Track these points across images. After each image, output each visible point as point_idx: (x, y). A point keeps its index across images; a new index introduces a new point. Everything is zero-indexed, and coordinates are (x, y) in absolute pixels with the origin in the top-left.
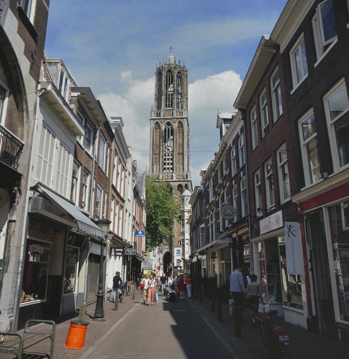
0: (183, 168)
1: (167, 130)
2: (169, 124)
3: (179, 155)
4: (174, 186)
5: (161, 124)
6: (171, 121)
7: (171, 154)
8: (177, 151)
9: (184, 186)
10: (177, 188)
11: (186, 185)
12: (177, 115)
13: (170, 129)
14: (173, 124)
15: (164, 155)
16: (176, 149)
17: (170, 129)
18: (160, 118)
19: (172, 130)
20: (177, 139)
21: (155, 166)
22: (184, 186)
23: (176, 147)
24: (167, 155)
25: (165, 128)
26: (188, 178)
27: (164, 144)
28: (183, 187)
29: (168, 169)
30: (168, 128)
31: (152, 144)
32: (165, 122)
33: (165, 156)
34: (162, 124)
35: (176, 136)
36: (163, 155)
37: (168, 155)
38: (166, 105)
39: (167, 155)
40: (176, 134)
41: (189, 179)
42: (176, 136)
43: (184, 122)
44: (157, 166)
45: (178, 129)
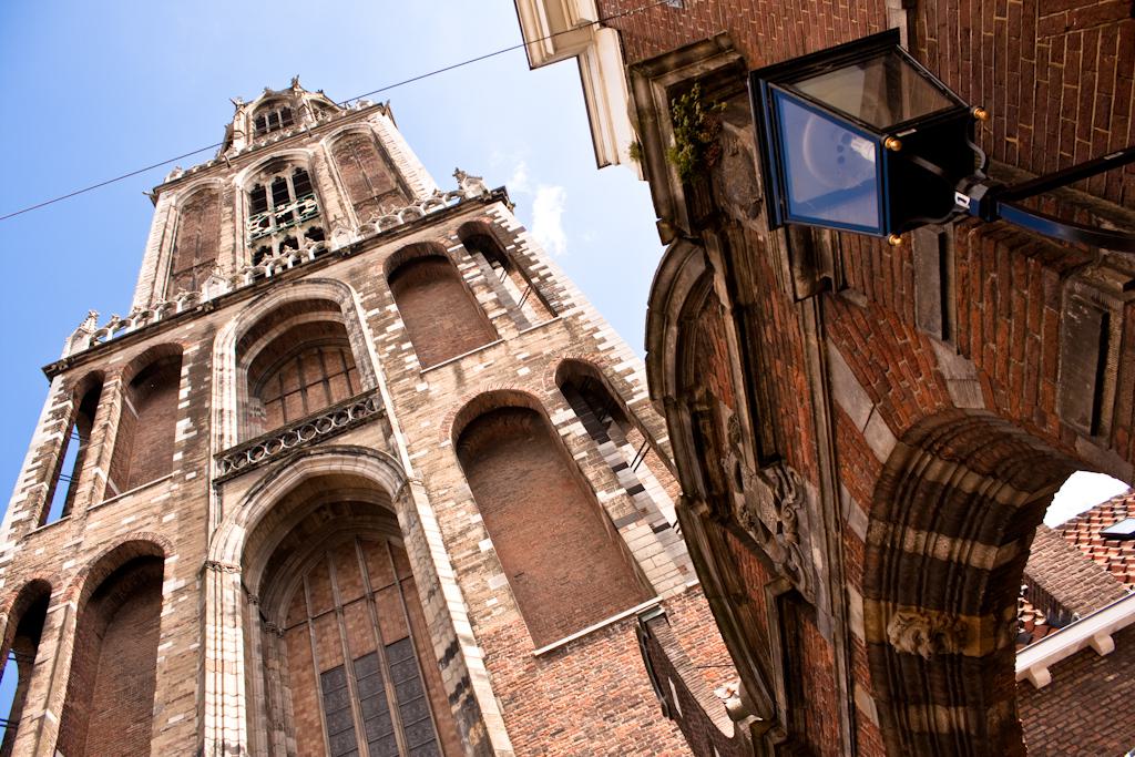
25: (257, 186)
32: (255, 164)
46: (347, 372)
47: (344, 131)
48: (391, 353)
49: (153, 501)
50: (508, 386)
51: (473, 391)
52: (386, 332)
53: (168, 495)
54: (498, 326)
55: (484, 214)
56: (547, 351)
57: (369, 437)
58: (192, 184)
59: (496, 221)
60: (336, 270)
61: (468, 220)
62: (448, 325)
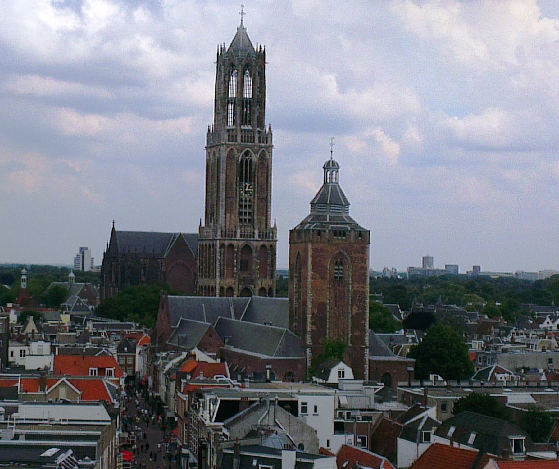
2: (247, 154)
4: (256, 247)
9: (268, 248)
12: (260, 142)
13: (249, 161)
14: (255, 154)
17: (249, 161)
18: (236, 143)
19: (251, 160)
22: (268, 248)
24: (244, 199)
26: (274, 238)
29: (245, 220)
37: (246, 201)
38: (242, 121)
39: (244, 199)
41: (275, 239)
51: (263, 286)
60: (255, 243)
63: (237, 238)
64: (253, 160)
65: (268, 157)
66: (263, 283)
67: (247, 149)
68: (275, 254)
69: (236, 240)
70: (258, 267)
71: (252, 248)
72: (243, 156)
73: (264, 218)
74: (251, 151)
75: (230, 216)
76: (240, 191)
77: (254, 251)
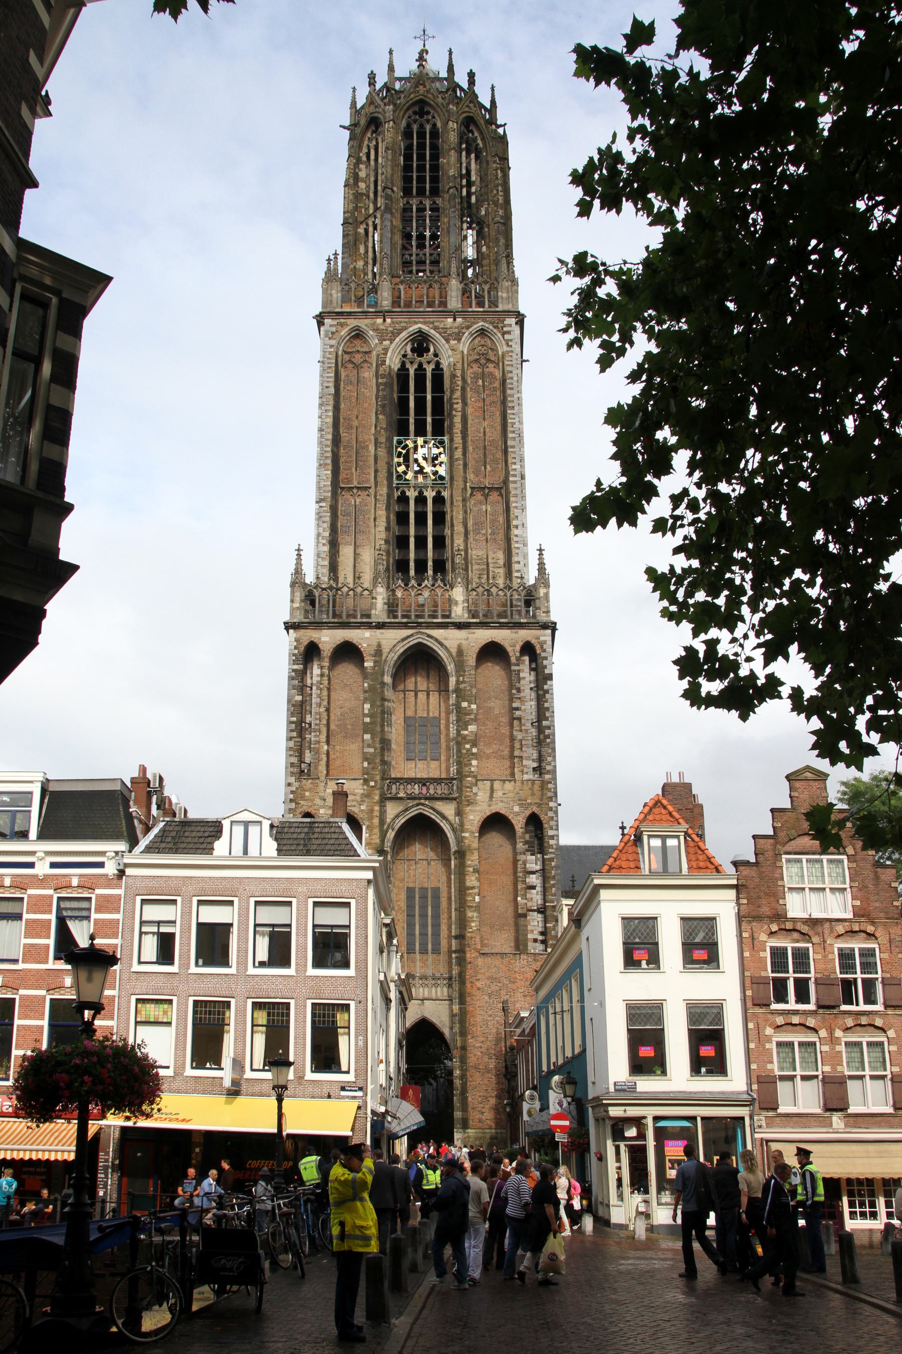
0: (508, 565)
1: (412, 372)
2: (421, 344)
3: (479, 496)
4: (460, 652)
5: (381, 340)
6: (435, 328)
7: (439, 493)
8: (471, 476)
10: (471, 660)
11: (528, 649)
13: (429, 369)
14: (447, 341)
15: (397, 494)
16: (465, 465)
17: (429, 369)
20: (470, 418)
21: (346, 552)
22: (513, 651)
23: (464, 454)
24: (412, 494)
25: (403, 364)
27: (395, 439)
28: (513, 660)
30: (420, 365)
31: (330, 437)
32: (404, 334)
33: (403, 499)
34: (386, 343)
35: (465, 403)
36: (389, 496)
37: (421, 500)
39: (412, 494)
40: (463, 389)
41: (542, 617)
42: (465, 403)
43: (504, 334)
44: (359, 551)
45: (475, 367)
46: (440, 691)
47: (482, 329)
48: (468, 750)
49: (356, 791)
50: (507, 814)
51: (495, 808)
52: (467, 729)
53: (362, 791)
54: (516, 765)
55: (538, 638)
56: (529, 801)
57: (448, 809)
58: (352, 323)
59: (543, 654)
60: (451, 638)
61: (529, 639)
62: (497, 711)
63: (374, 620)
64: (445, 364)
65: (502, 349)
66: (498, 794)
67: (415, 327)
68: (550, 677)
69: (369, 626)
70: (472, 728)
71: (442, 653)
72: (405, 356)
73: (501, 556)
74: (432, 331)
75: (356, 555)
76: (390, 465)
77: (451, 667)
